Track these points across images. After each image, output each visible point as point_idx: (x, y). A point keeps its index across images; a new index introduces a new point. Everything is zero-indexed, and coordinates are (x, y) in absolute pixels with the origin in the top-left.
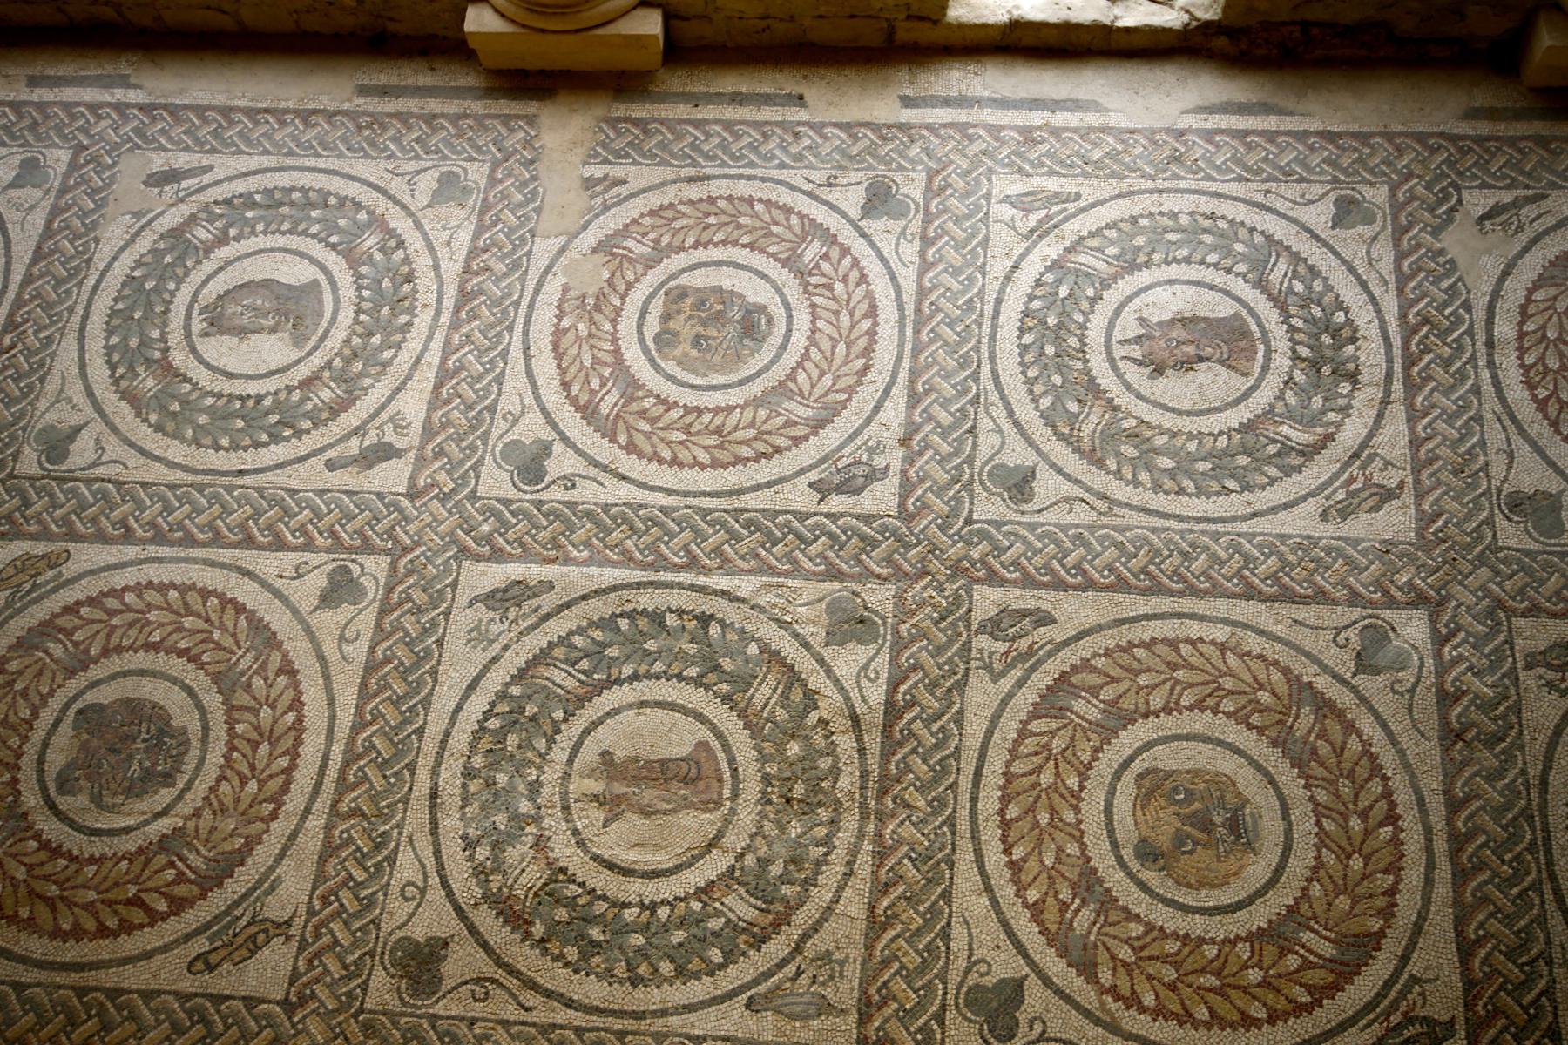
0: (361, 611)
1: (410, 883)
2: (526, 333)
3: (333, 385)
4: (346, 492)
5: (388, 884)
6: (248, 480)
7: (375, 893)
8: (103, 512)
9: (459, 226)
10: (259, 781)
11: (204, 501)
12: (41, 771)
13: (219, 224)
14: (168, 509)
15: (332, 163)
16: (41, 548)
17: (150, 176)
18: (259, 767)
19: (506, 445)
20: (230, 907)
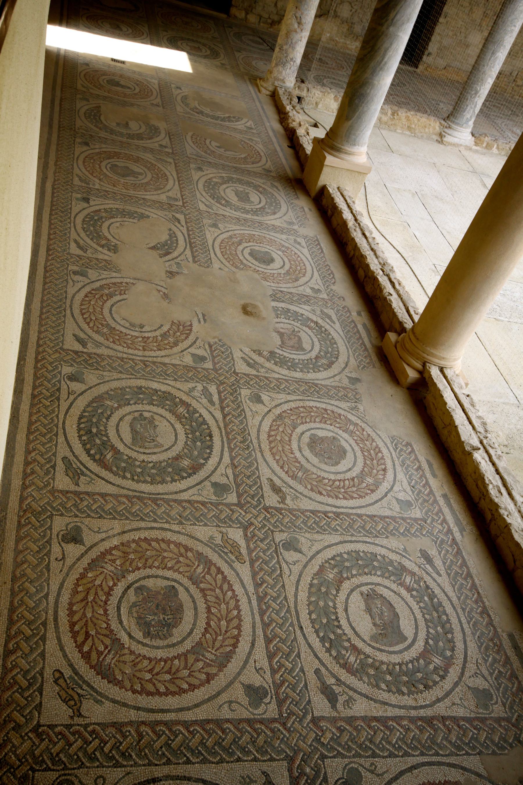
0: (246, 709)
1: (104, 780)
2: (423, 764)
3: (358, 661)
4: (306, 683)
5: (103, 767)
6: (298, 632)
7: (98, 760)
8: (266, 572)
9: (465, 707)
10: (151, 679)
11: (283, 614)
12: (144, 578)
13: (415, 586)
14: (275, 599)
15: (468, 631)
16: (244, 551)
17: (425, 551)
18: (158, 677)
19: (357, 769)
20: (87, 682)
